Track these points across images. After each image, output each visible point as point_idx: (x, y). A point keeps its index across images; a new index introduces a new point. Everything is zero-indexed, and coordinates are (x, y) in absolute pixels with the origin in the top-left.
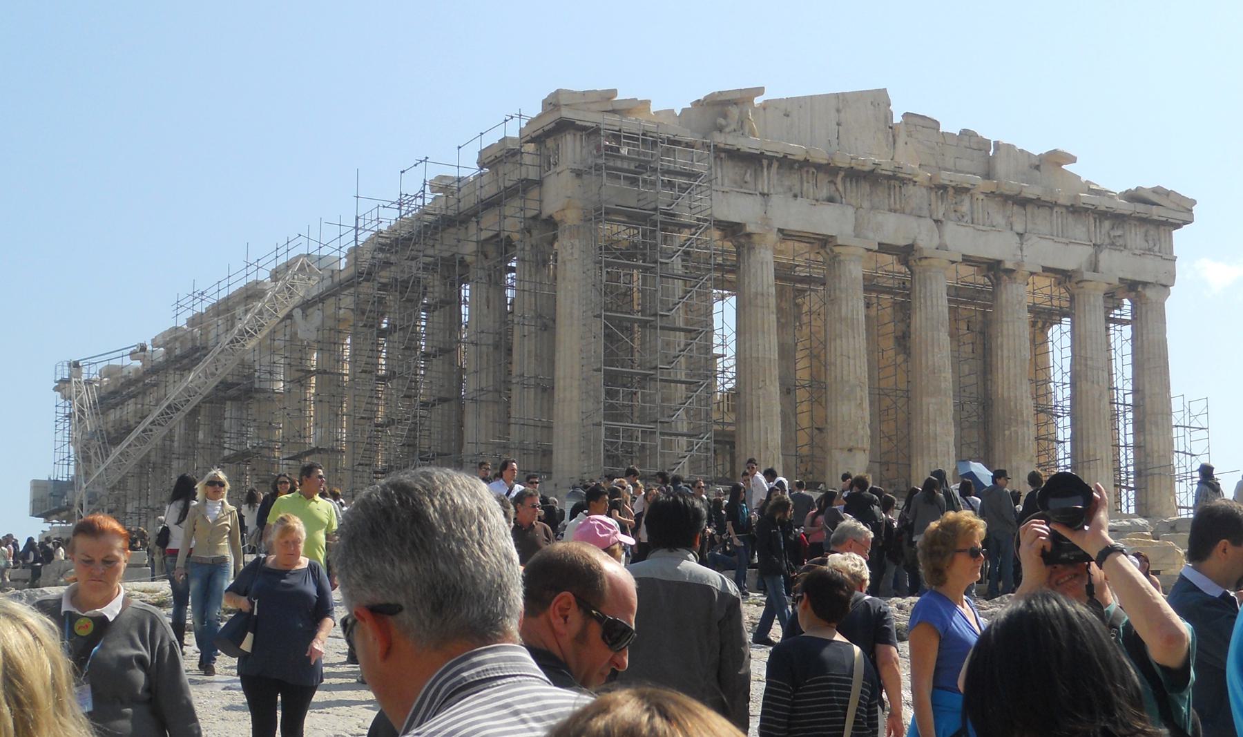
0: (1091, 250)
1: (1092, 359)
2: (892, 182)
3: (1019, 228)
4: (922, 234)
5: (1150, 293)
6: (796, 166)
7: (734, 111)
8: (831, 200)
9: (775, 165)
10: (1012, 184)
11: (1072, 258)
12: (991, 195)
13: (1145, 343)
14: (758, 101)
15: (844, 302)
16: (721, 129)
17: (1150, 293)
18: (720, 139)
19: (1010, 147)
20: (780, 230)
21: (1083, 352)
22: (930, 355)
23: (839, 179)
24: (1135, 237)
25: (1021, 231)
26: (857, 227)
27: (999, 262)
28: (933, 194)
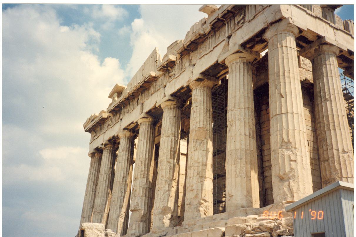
20: (124, 129)
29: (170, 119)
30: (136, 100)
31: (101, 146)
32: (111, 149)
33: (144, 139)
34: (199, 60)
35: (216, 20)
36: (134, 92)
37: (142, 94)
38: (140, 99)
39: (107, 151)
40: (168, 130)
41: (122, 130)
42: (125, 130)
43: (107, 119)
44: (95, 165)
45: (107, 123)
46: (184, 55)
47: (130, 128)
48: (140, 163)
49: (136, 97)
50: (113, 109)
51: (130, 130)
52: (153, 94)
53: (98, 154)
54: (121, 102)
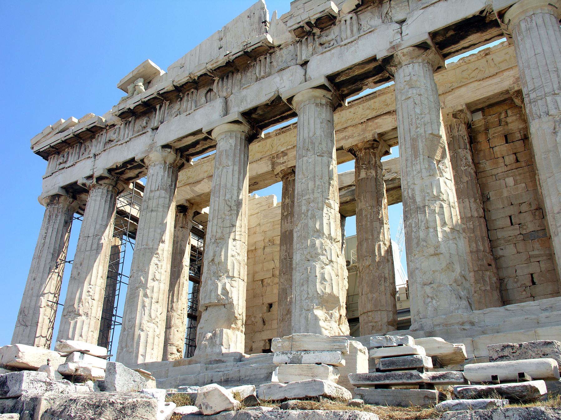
20: (164, 147)
25: (400, 17)
29: (321, 123)
30: (203, 91)
31: (85, 181)
32: (111, 189)
33: (234, 164)
34: (422, 11)
36: (205, 74)
37: (225, 80)
38: (215, 90)
39: (100, 190)
40: (320, 143)
41: (160, 147)
42: (166, 149)
43: (105, 131)
44: (58, 221)
45: (104, 137)
46: (366, 6)
47: (178, 147)
48: (227, 208)
49: (204, 87)
50: (132, 108)
51: (177, 150)
52: (263, 78)
53: (65, 200)
54: (161, 92)
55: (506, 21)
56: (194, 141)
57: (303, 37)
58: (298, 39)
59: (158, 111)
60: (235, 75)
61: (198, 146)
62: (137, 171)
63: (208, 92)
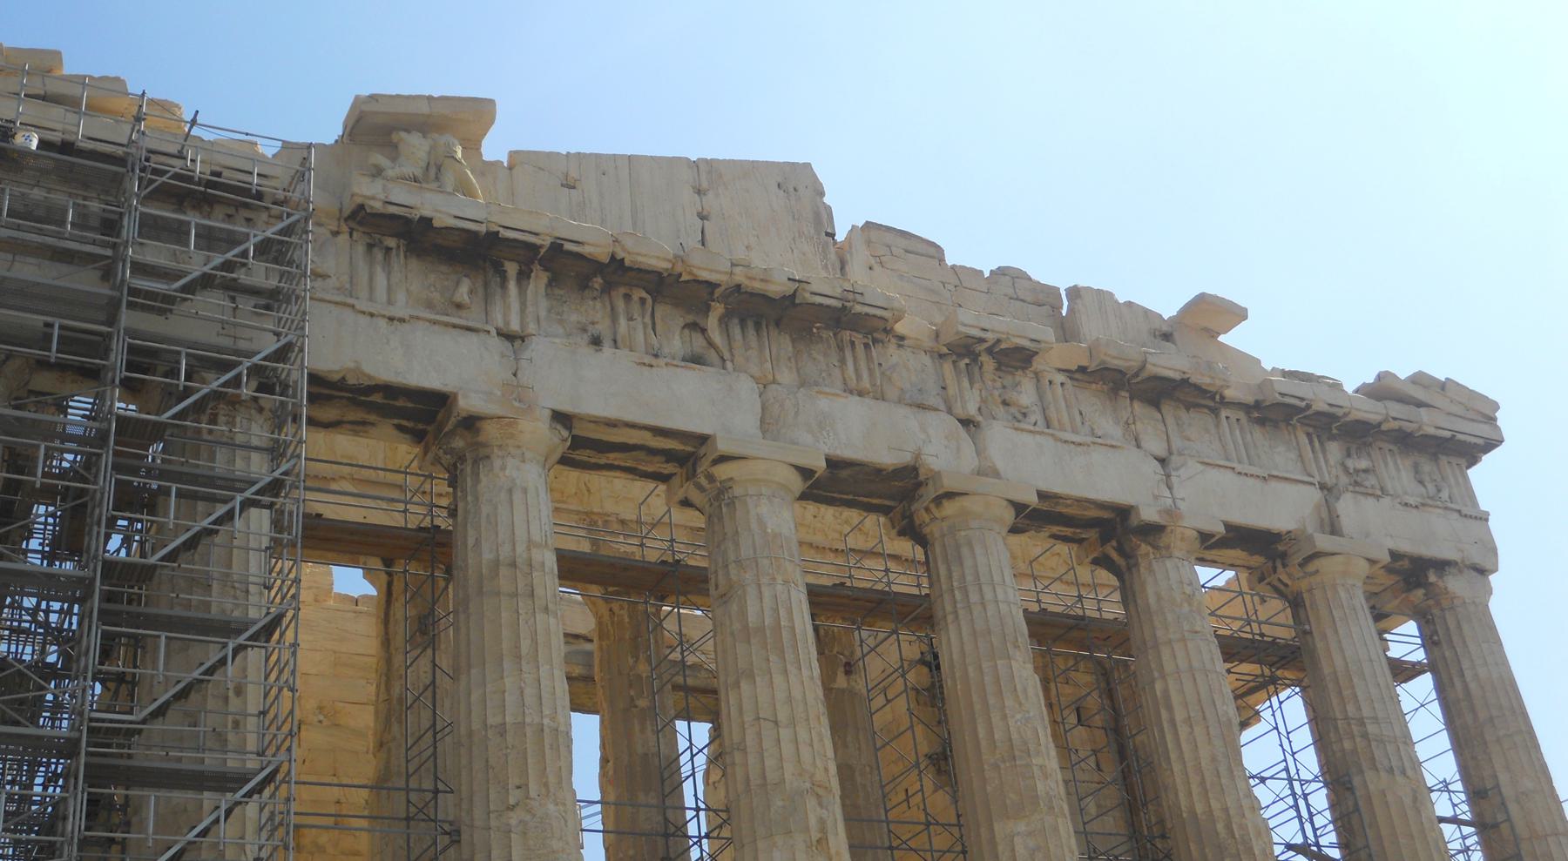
0: (1315, 495)
1: (1375, 720)
2: (846, 335)
3: (1159, 449)
4: (939, 448)
5: (1455, 584)
6: (598, 282)
7: (416, 147)
8: (696, 360)
9: (539, 279)
10: (1125, 352)
11: (1283, 508)
12: (1080, 375)
13: (1473, 686)
14: (494, 148)
15: (751, 592)
16: (378, 172)
17: (1455, 584)
18: (372, 192)
19: (1103, 297)
20: (561, 418)
21: (1351, 709)
22: (996, 719)
23: (712, 323)
24: (1397, 472)
25: (1162, 453)
26: (767, 424)
27: (1123, 512)
28: (948, 367)
34: (1201, 467)
35: (1303, 404)
36: (711, 286)
41: (547, 413)
42: (559, 427)
54: (568, 246)
55: (1311, 568)
56: (631, 442)
57: (961, 356)
58: (945, 350)
59: (512, 286)
60: (774, 332)
61: (612, 456)
62: (359, 415)
63: (686, 326)
